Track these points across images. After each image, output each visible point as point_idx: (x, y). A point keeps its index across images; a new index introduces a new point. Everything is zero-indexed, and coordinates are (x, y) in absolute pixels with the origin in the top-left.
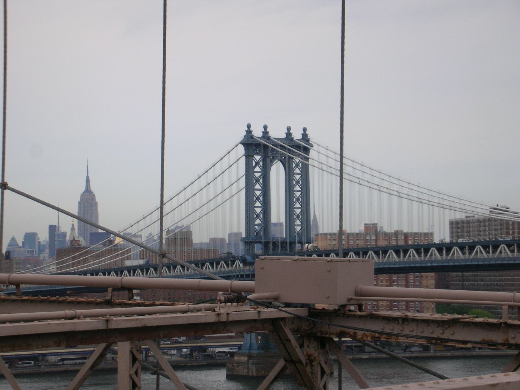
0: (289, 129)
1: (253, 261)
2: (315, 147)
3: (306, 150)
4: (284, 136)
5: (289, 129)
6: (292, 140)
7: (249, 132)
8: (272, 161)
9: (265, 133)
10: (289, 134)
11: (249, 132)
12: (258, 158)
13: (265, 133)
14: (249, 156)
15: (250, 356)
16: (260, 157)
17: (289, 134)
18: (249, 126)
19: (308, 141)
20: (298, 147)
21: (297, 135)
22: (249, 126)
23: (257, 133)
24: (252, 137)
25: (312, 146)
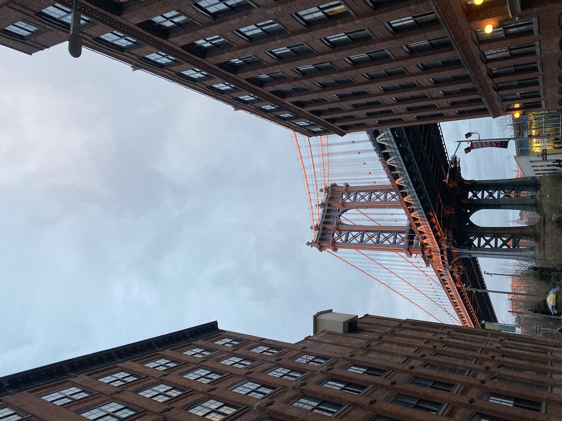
18: (308, 244)
21: (322, 197)
22: (308, 244)
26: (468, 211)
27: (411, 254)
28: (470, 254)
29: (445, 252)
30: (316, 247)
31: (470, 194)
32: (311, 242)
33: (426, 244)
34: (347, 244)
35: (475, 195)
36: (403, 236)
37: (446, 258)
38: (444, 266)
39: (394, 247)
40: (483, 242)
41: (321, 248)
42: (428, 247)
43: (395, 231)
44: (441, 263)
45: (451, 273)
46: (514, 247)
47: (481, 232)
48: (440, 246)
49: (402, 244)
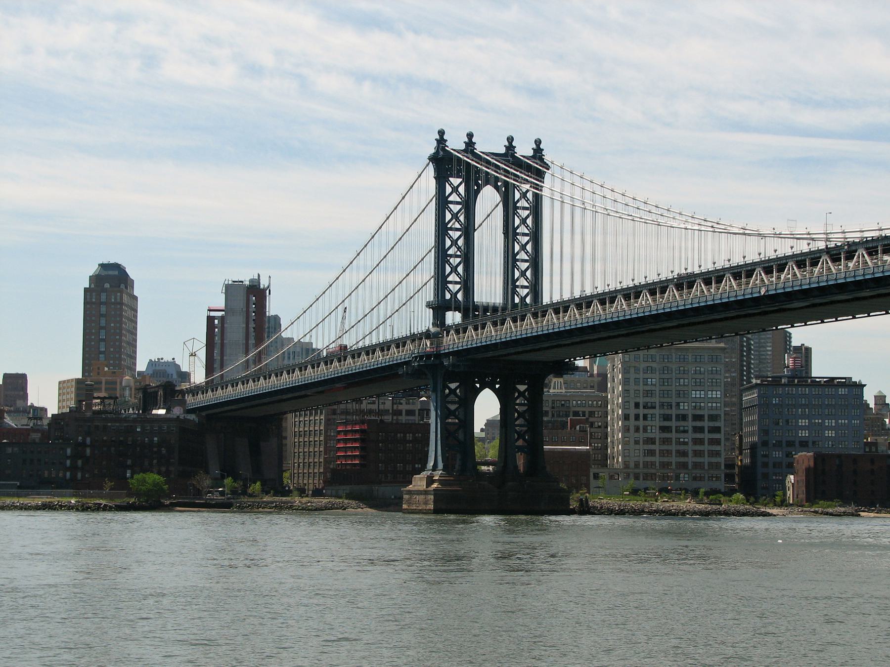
0: (510, 140)
2: (554, 169)
3: (540, 175)
4: (502, 150)
5: (510, 140)
6: (513, 156)
7: (441, 141)
9: (470, 144)
10: (510, 148)
11: (441, 141)
12: (456, 181)
13: (470, 144)
14: (441, 179)
16: (460, 180)
17: (510, 148)
18: (441, 133)
19: (541, 159)
20: (528, 168)
21: (524, 150)
22: (441, 133)
23: (455, 143)
24: (444, 150)
26: (497, 386)
27: (433, 308)
29: (437, 362)
30: (438, 148)
31: (522, 388)
32: (445, 137)
34: (442, 202)
35: (521, 394)
36: (460, 296)
38: (416, 357)
39: (441, 281)
40: (453, 407)
41: (434, 159)
43: (467, 284)
45: (407, 363)
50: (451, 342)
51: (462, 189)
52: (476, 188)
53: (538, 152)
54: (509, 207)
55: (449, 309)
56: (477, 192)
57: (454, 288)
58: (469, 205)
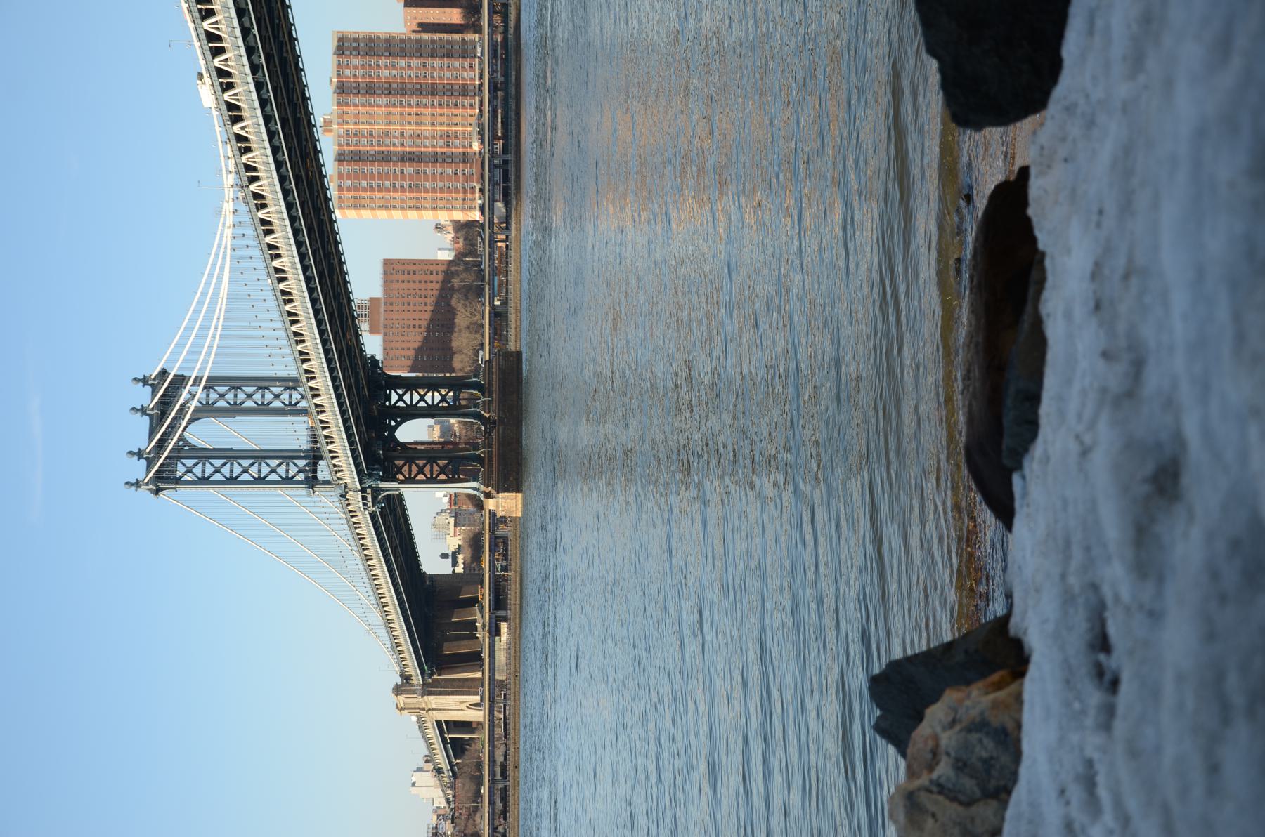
1: (343, 486)
7: (137, 484)
8: (187, 443)
11: (137, 484)
12: (181, 470)
15: (488, 495)
17: (143, 410)
21: (144, 397)
23: (138, 469)
25: (164, 373)
26: (393, 423)
28: (398, 489)
29: (369, 490)
31: (394, 397)
33: (339, 479)
35: (401, 398)
36: (301, 463)
37: (369, 498)
42: (341, 482)
43: (287, 456)
44: (361, 504)
46: (454, 477)
47: (411, 452)
48: (361, 484)
49: (301, 477)
50: (349, 475)
51: (190, 463)
52: (187, 448)
53: (145, 381)
54: (206, 411)
55: (315, 478)
56: (194, 448)
57: (293, 470)
58: (203, 455)
